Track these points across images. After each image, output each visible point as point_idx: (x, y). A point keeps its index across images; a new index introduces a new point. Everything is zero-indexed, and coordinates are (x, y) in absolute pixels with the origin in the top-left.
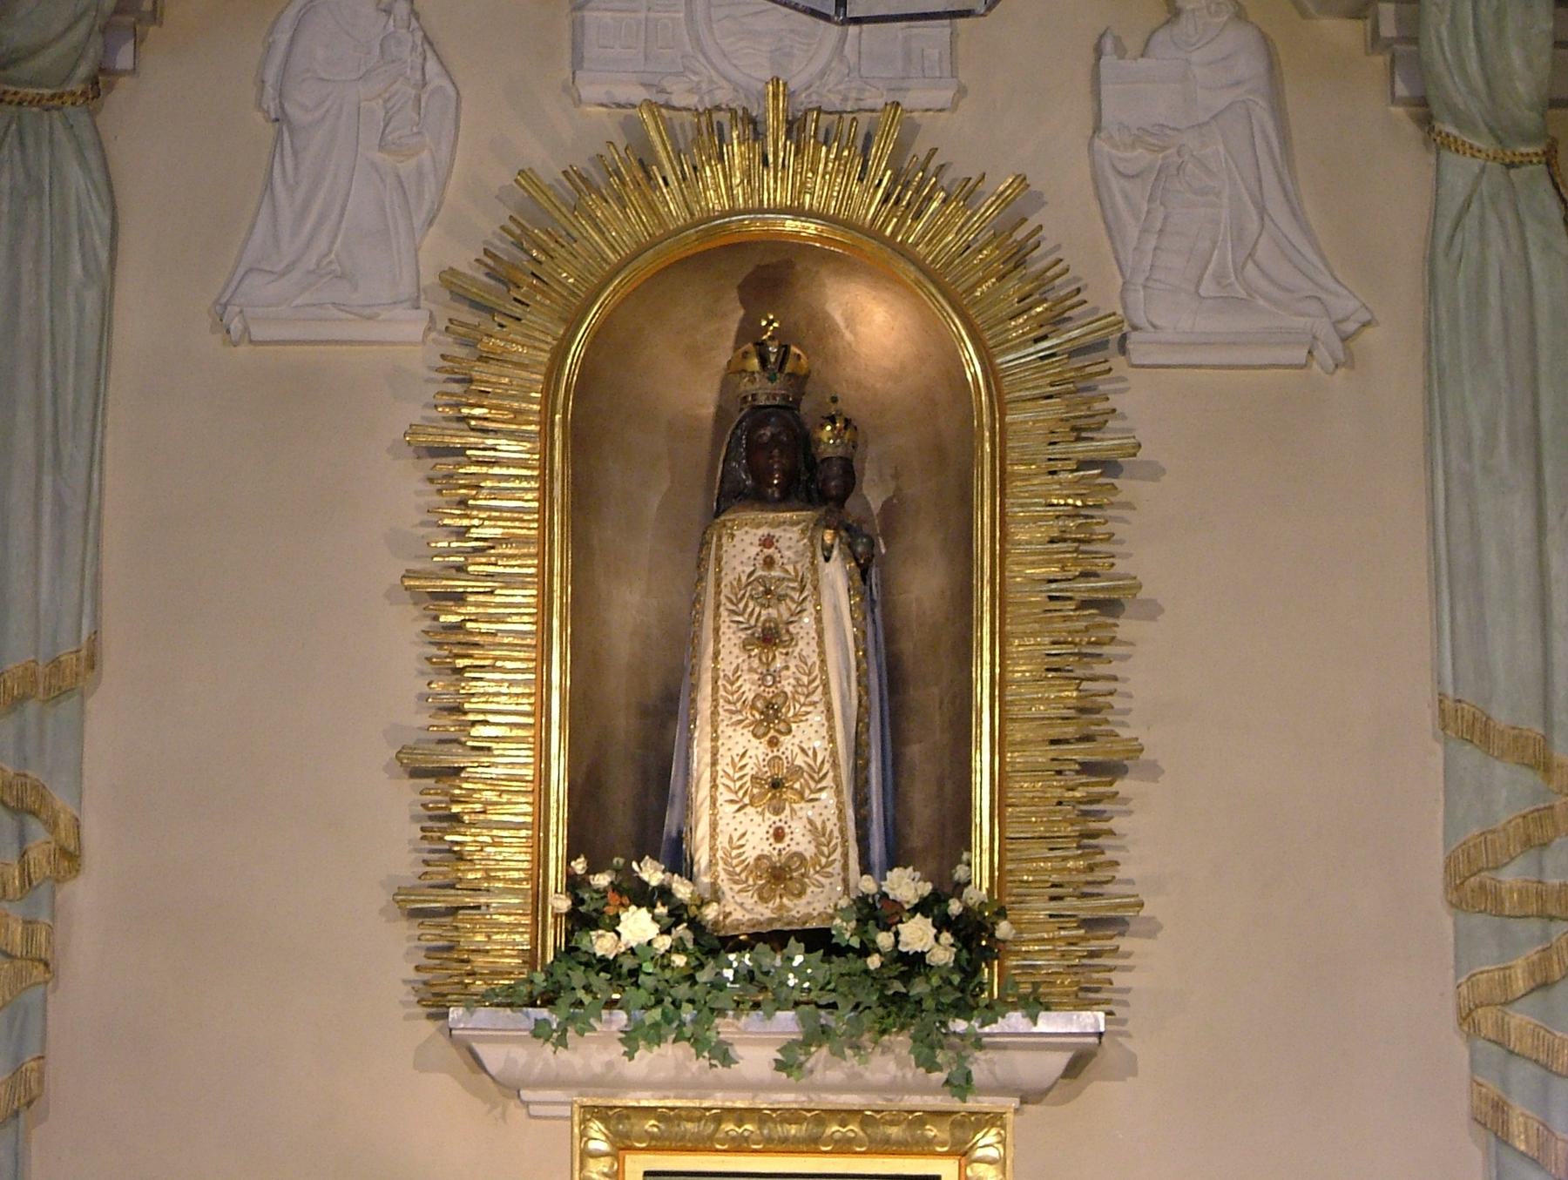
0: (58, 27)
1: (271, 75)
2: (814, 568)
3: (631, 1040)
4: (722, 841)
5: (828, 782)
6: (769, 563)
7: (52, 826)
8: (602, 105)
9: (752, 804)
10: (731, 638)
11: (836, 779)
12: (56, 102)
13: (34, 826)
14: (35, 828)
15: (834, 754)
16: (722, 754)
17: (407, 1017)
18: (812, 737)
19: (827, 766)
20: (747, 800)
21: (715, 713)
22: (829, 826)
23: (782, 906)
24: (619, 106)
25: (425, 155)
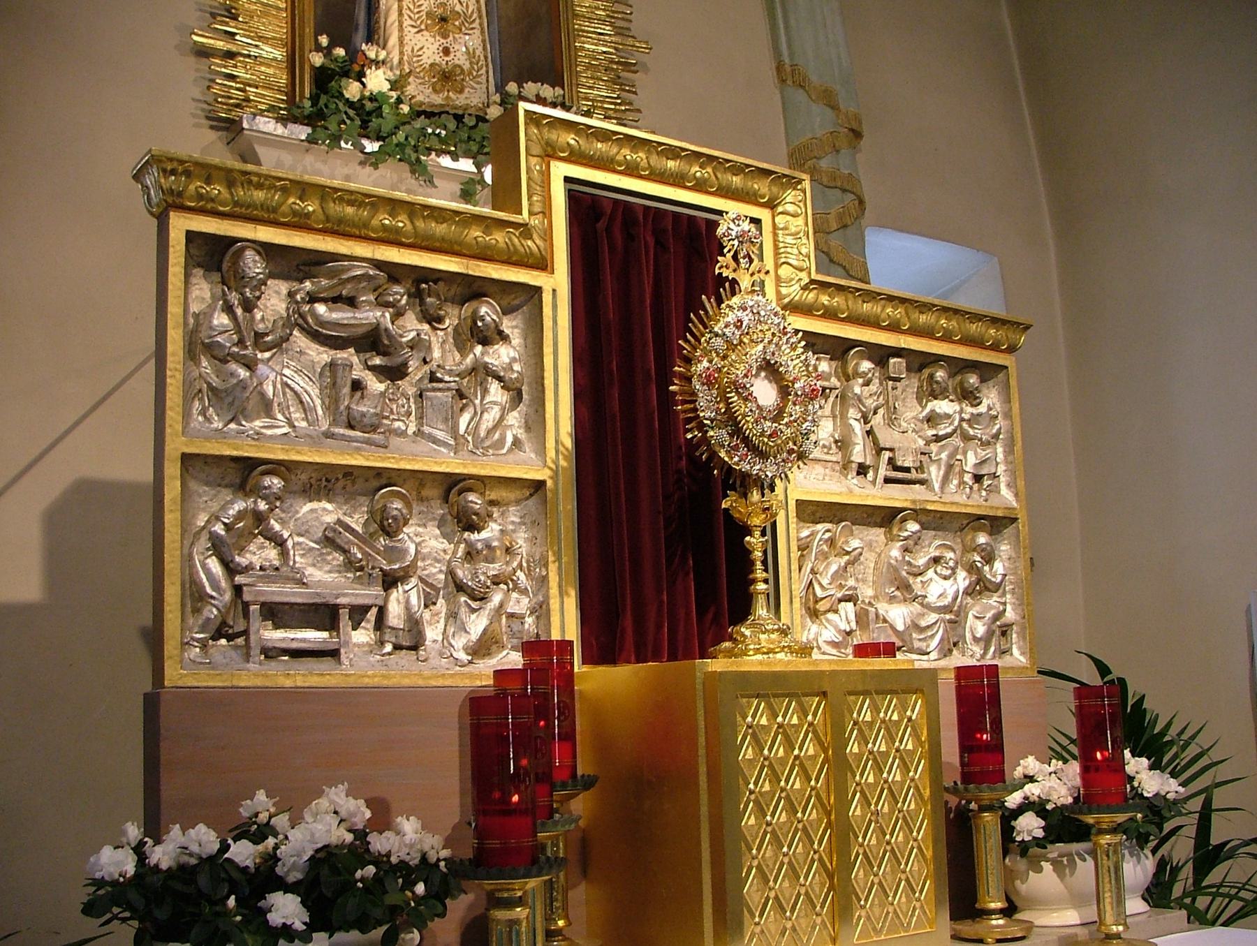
3: (372, 161)
4: (407, 49)
5: (476, 25)
9: (427, 29)
11: (481, 24)
15: (479, 11)
17: (196, 125)
19: (475, 15)
20: (423, 27)
22: (478, 53)
23: (448, 97)
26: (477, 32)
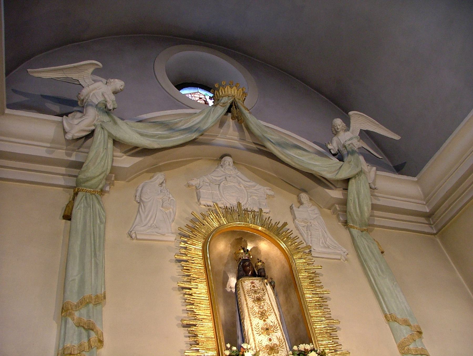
0: (98, 174)
1: (138, 194)
2: (265, 287)
4: (257, 342)
5: (278, 328)
6: (254, 287)
7: (97, 333)
8: (205, 205)
9: (262, 333)
10: (250, 301)
11: (280, 328)
12: (94, 192)
13: (92, 333)
14: (92, 333)
15: (279, 323)
16: (252, 324)
18: (273, 319)
19: (278, 325)
20: (261, 333)
21: (249, 315)
22: (281, 338)
24: (208, 206)
25: (171, 210)
26: (279, 331)
